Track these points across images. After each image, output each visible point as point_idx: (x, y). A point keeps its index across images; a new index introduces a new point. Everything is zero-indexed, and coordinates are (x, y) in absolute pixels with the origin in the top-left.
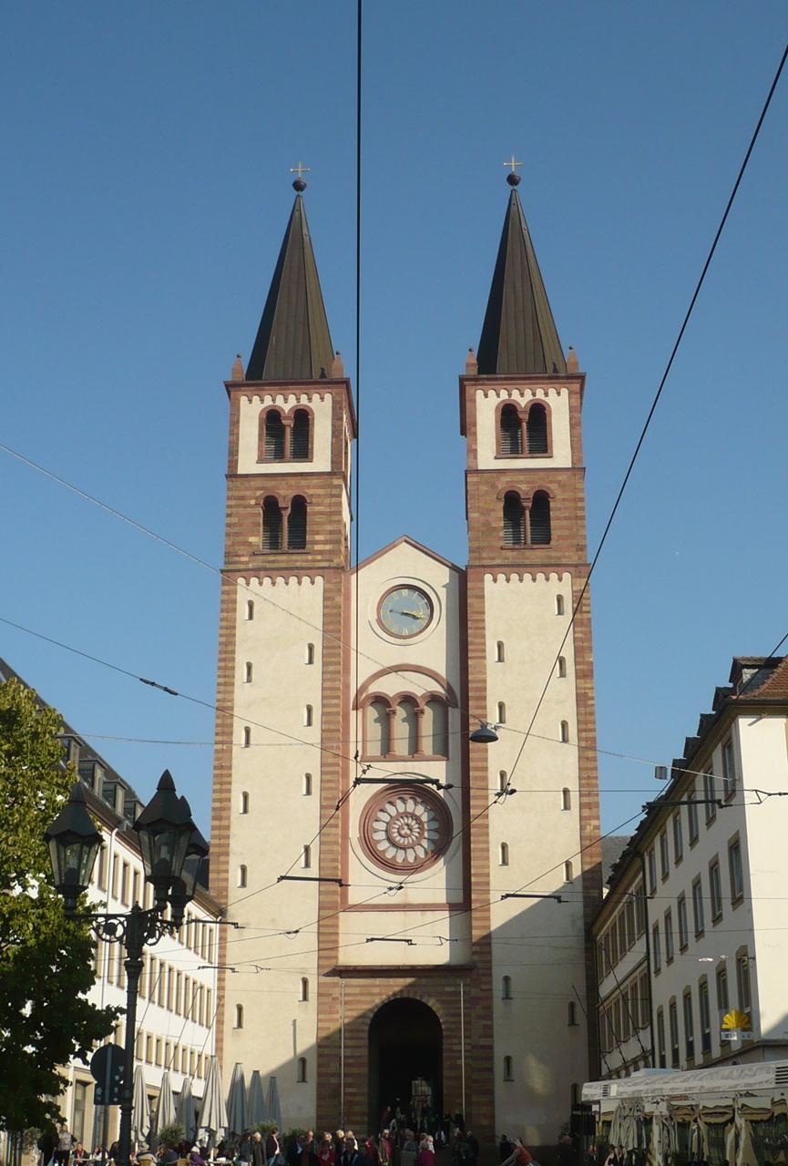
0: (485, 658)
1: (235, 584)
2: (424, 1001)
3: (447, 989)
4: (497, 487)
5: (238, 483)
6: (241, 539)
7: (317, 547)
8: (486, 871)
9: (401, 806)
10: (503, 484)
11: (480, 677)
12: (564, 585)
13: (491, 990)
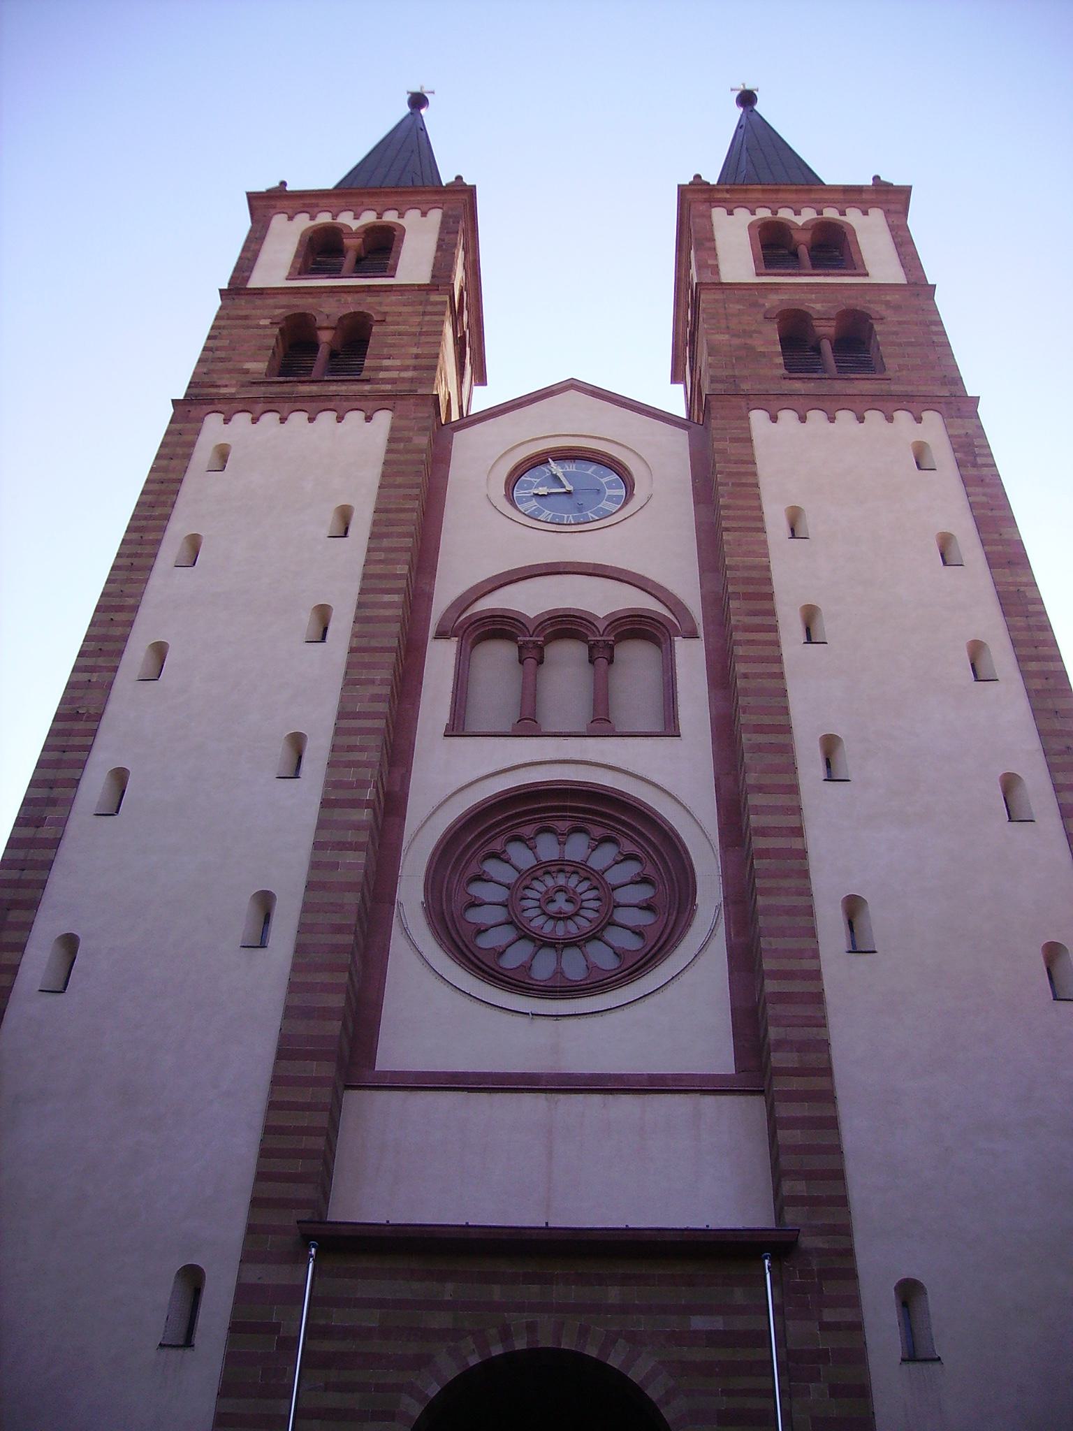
0: (762, 530)
1: (202, 420)
2: (614, 1362)
3: (699, 1323)
4: (764, 305)
5: (242, 301)
6: (230, 365)
7: (382, 375)
8: (807, 964)
9: (548, 848)
10: (772, 301)
11: (750, 560)
12: (933, 429)
13: (857, 1327)
